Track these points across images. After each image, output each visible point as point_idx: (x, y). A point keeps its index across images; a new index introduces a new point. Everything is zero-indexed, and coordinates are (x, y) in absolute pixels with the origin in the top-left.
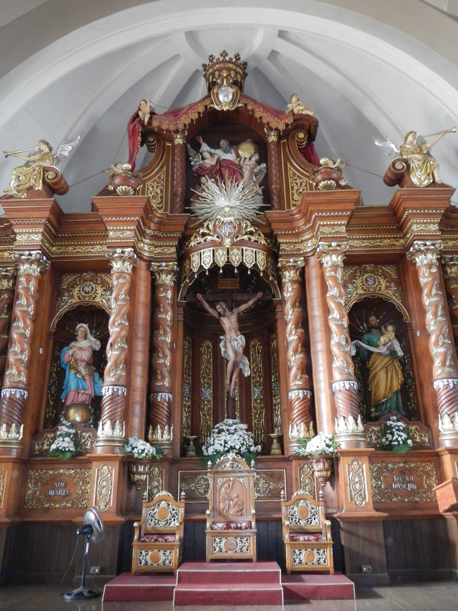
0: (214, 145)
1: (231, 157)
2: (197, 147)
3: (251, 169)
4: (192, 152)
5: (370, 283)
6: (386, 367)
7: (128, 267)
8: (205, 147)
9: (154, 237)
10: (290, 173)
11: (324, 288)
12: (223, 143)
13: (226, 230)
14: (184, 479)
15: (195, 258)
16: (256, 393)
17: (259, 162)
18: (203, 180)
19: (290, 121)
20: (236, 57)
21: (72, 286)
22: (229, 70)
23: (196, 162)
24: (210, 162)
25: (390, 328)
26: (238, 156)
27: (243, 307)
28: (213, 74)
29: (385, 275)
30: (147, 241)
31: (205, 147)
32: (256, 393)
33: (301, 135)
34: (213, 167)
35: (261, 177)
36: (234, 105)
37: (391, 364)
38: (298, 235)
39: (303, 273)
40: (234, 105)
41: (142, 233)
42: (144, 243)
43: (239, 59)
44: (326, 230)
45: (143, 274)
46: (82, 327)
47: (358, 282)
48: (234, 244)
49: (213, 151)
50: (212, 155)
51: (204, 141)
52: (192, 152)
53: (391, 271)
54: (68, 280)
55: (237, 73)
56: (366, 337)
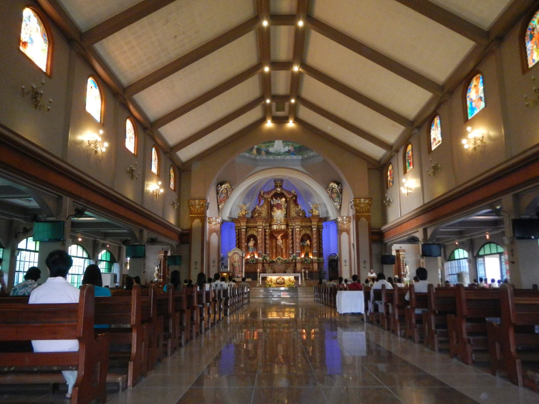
0: (276, 199)
1: (279, 202)
2: (272, 199)
4: (271, 200)
6: (307, 248)
7: (261, 230)
8: (274, 199)
9: (265, 222)
10: (292, 206)
11: (296, 234)
12: (278, 199)
13: (279, 222)
14: (271, 266)
15: (273, 226)
16: (284, 250)
17: (285, 203)
18: (274, 207)
19: (292, 195)
21: (249, 230)
22: (279, 183)
23: (272, 203)
24: (275, 203)
25: (308, 240)
26: (281, 201)
27: (281, 234)
28: (276, 183)
29: (309, 229)
32: (284, 250)
33: (294, 198)
34: (276, 204)
35: (286, 207)
38: (293, 222)
39: (293, 229)
41: (263, 222)
44: (297, 223)
45: (263, 230)
46: (252, 239)
47: (303, 231)
48: (280, 225)
49: (276, 200)
50: (276, 201)
52: (271, 200)
53: (310, 229)
54: (248, 230)
55: (281, 183)
56: (304, 241)
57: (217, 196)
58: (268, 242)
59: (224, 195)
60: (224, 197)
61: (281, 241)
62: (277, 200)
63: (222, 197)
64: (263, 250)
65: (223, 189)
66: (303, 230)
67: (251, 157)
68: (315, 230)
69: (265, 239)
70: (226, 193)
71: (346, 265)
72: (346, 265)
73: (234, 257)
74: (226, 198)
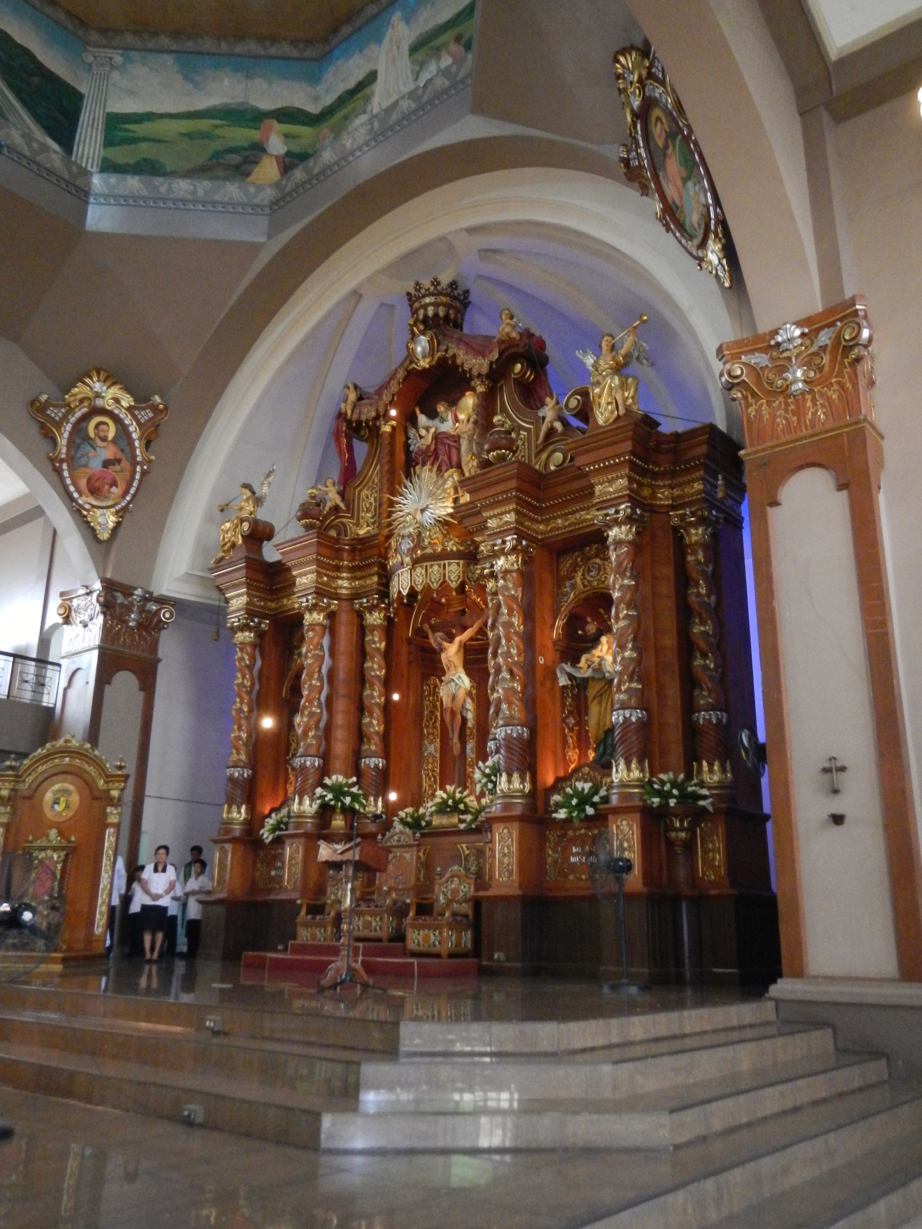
0: (432, 414)
1: (447, 427)
3: (469, 436)
5: (592, 574)
12: (441, 408)
20: (433, 284)
30: (345, 575)
31: (422, 419)
36: (433, 356)
37: (606, 691)
40: (433, 356)
42: (342, 579)
43: (439, 284)
51: (422, 412)
57: (52, 460)
58: (375, 695)
59: (108, 452)
60: (107, 464)
61: (466, 682)
62: (436, 422)
63: (96, 465)
64: (340, 748)
65: (86, 418)
66: (575, 568)
67: (217, 198)
68: (618, 543)
69: (361, 679)
70: (115, 441)
71: (838, 819)
72: (838, 819)
73: (49, 796)
74: (125, 464)
